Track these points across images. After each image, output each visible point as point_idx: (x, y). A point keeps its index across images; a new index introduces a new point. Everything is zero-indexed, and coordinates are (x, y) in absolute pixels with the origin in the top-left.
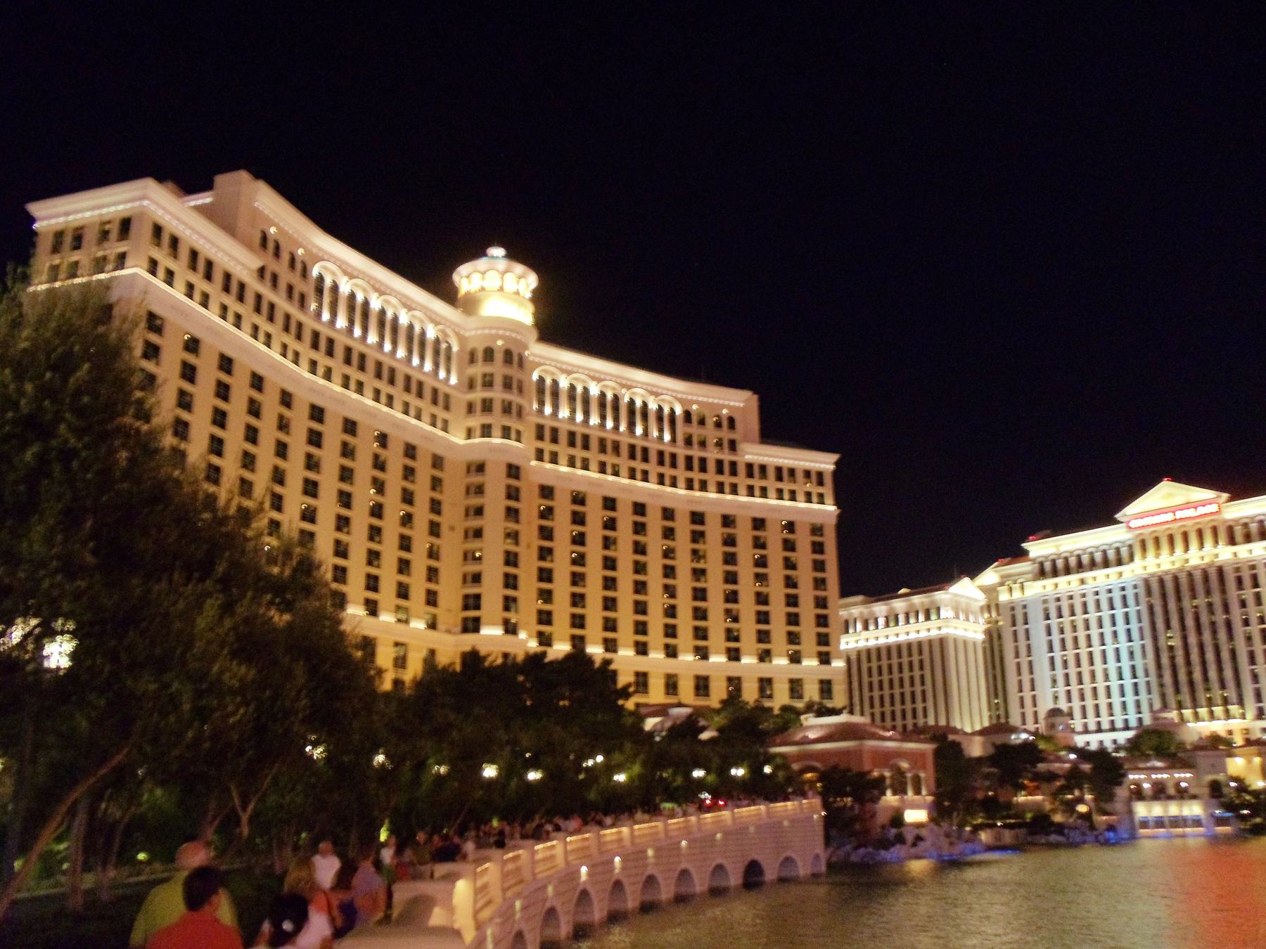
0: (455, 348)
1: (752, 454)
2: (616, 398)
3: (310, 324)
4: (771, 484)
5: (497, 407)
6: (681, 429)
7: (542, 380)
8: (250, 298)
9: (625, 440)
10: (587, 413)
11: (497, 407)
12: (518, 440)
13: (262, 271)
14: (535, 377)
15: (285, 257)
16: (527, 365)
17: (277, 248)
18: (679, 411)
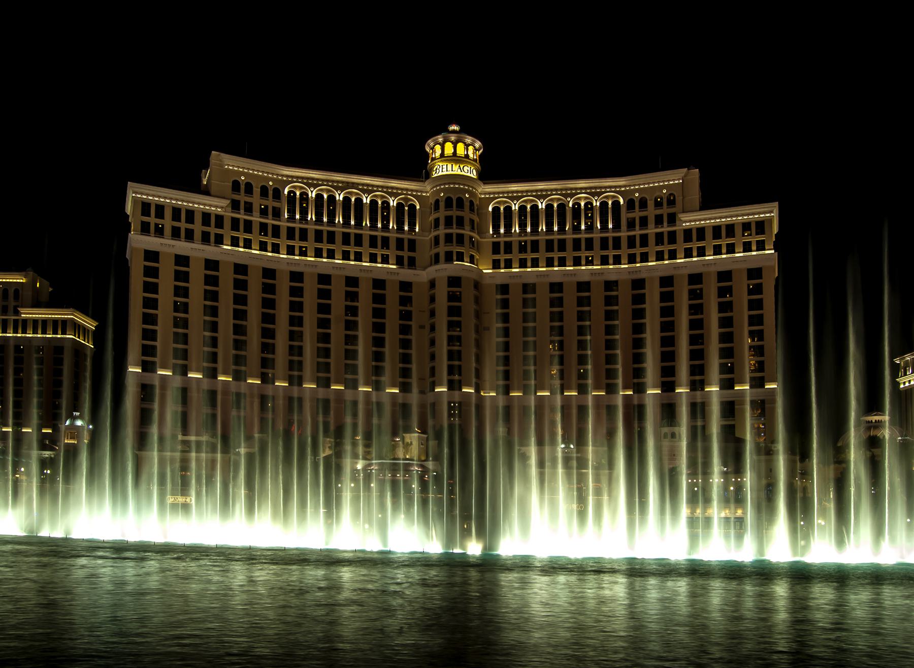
0: (418, 207)
1: (690, 221)
2: (562, 207)
3: (284, 224)
4: (710, 243)
5: (442, 240)
6: (624, 216)
7: (496, 210)
8: (227, 224)
9: (569, 237)
10: (535, 226)
11: (442, 240)
12: (460, 257)
13: (235, 205)
14: (490, 209)
15: (257, 191)
16: (467, 204)
17: (249, 188)
18: (621, 201)
